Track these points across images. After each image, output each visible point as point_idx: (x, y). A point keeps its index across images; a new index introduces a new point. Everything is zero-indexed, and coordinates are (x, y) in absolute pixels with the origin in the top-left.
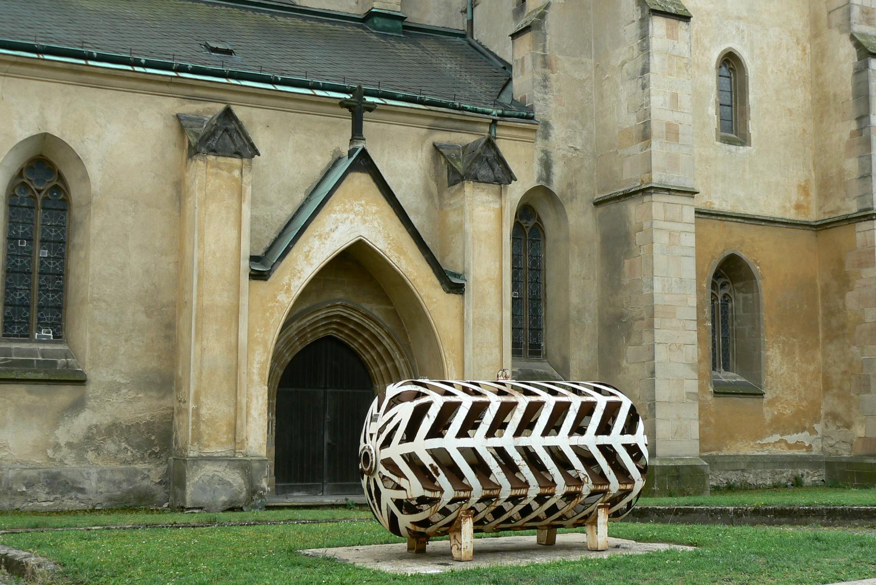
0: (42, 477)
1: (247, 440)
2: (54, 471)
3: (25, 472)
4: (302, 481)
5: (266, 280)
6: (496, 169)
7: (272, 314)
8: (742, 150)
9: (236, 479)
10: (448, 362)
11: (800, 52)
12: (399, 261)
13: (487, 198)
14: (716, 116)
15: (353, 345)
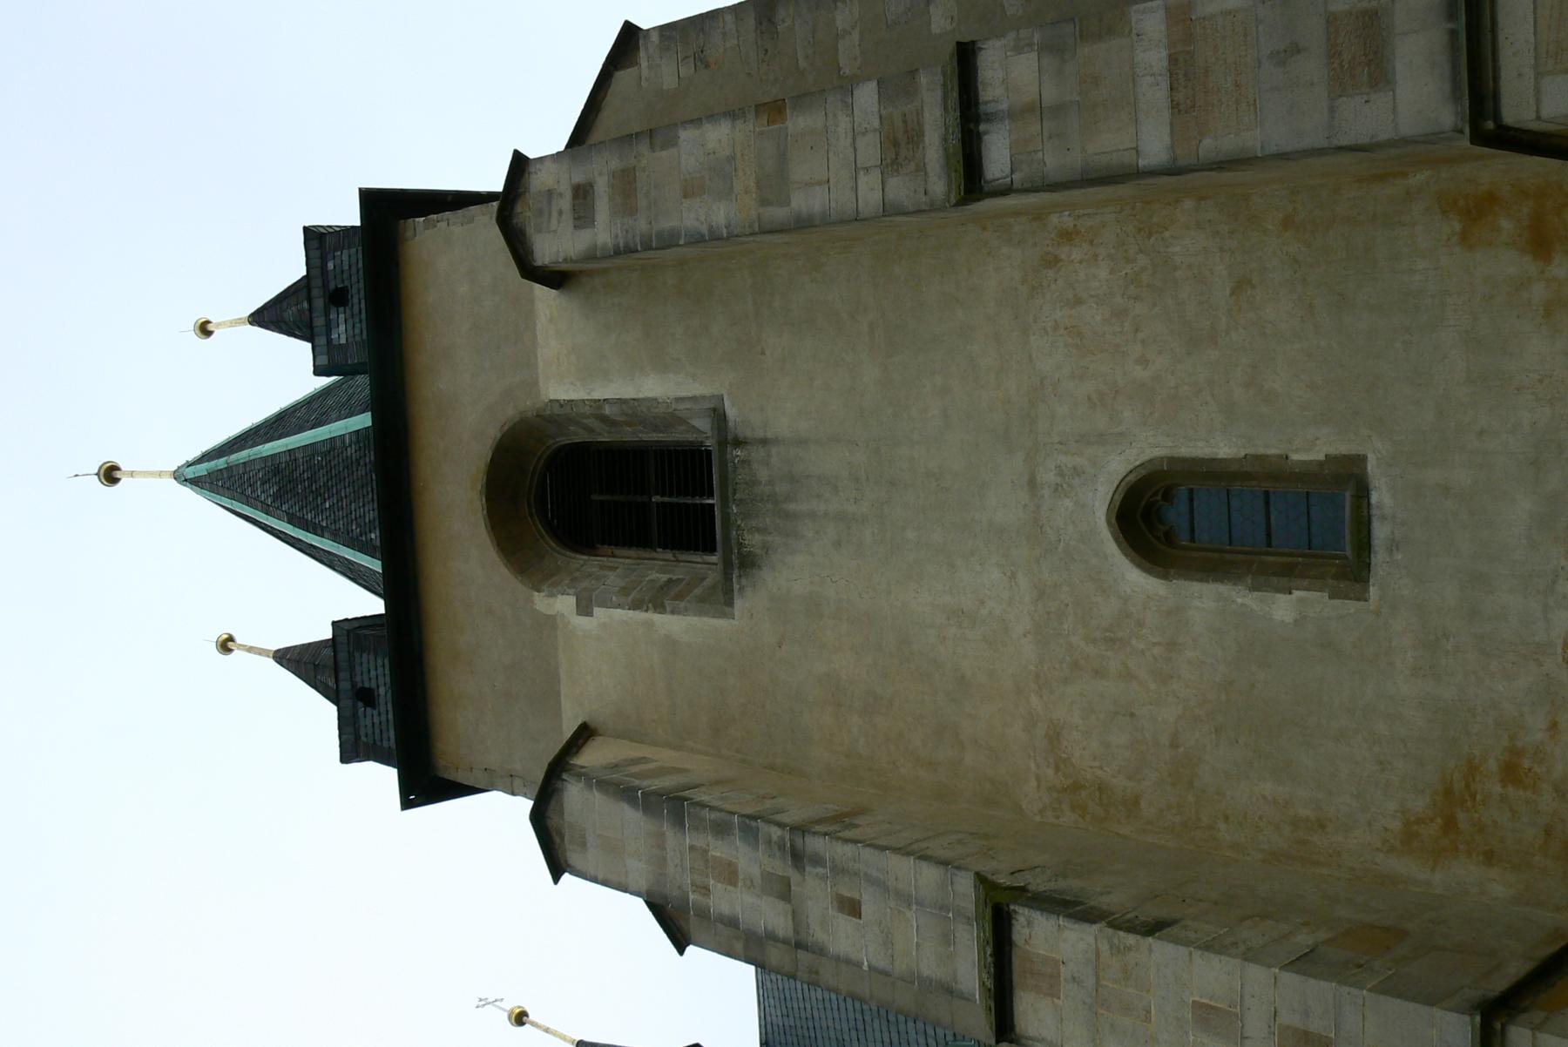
8: (1381, 496)
11: (1077, 254)
14: (1297, 594)
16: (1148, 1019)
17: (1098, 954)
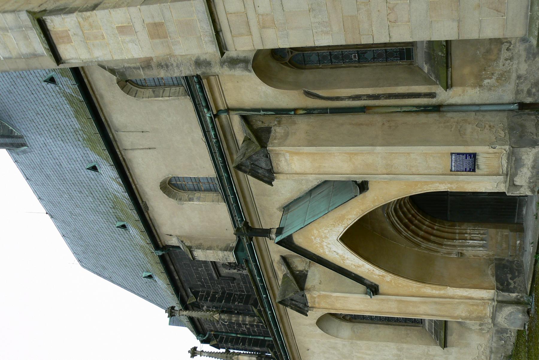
0: (497, 335)
1: (483, 298)
2: (494, 331)
3: (494, 340)
4: (515, 209)
5: (378, 286)
6: (258, 158)
7: (399, 284)
9: (508, 310)
10: (425, 189)
12: (350, 219)
13: (283, 162)
15: (415, 212)
16: (104, 38)
17: (79, 23)
